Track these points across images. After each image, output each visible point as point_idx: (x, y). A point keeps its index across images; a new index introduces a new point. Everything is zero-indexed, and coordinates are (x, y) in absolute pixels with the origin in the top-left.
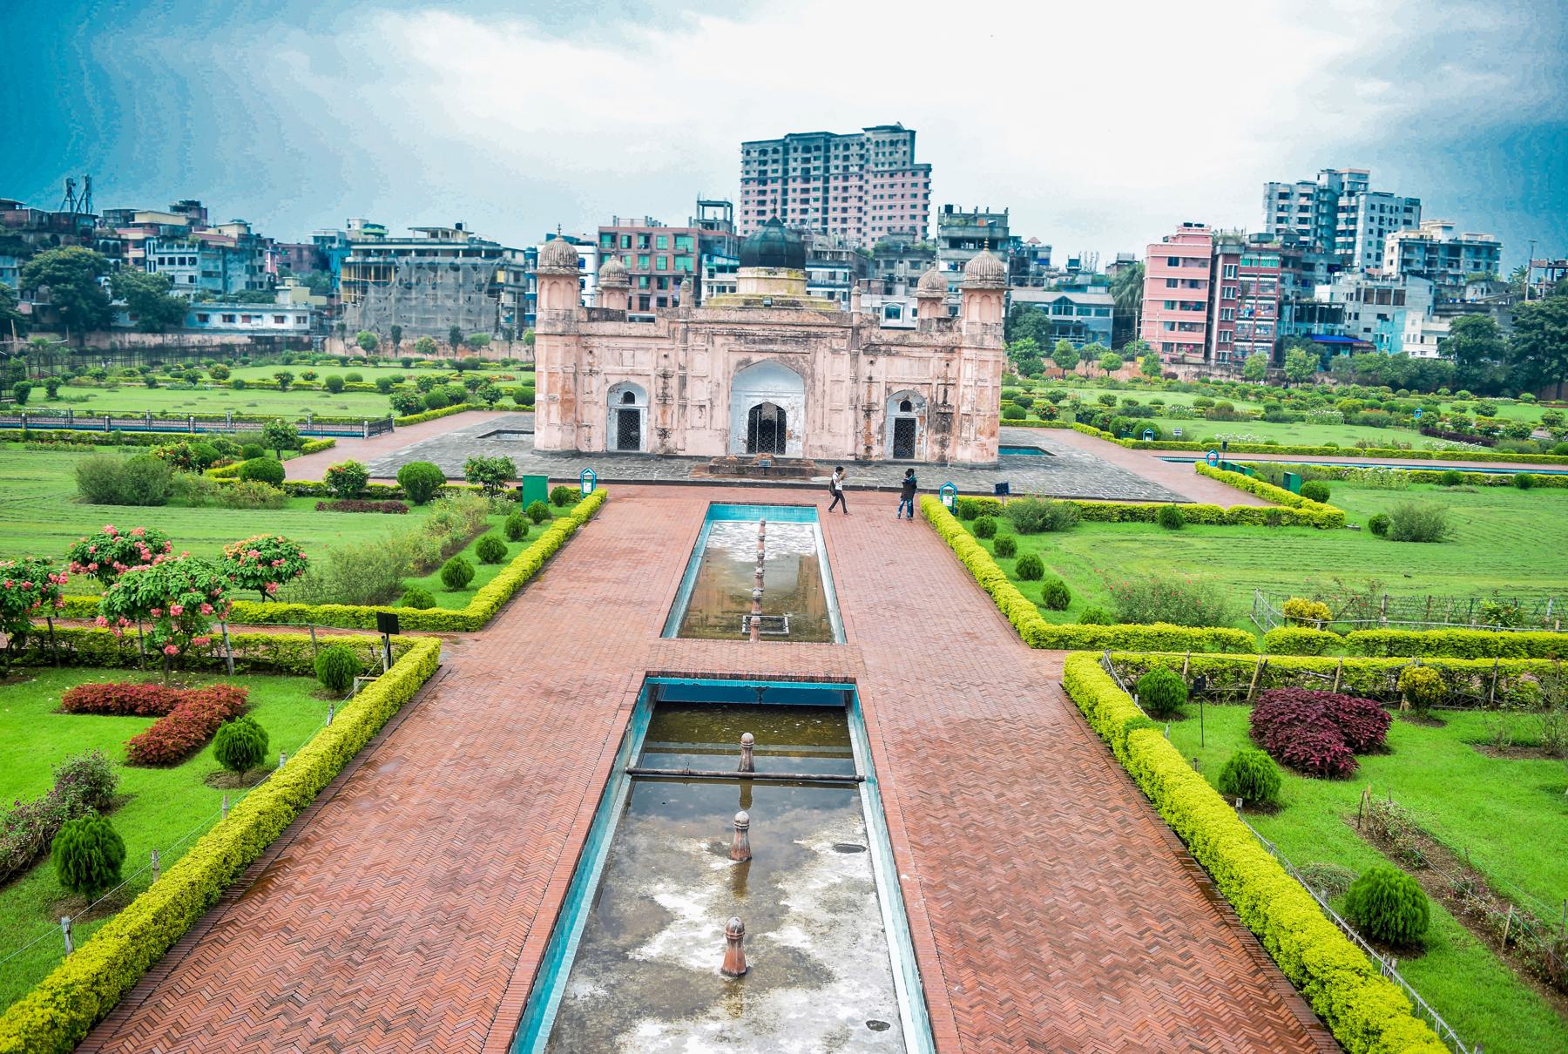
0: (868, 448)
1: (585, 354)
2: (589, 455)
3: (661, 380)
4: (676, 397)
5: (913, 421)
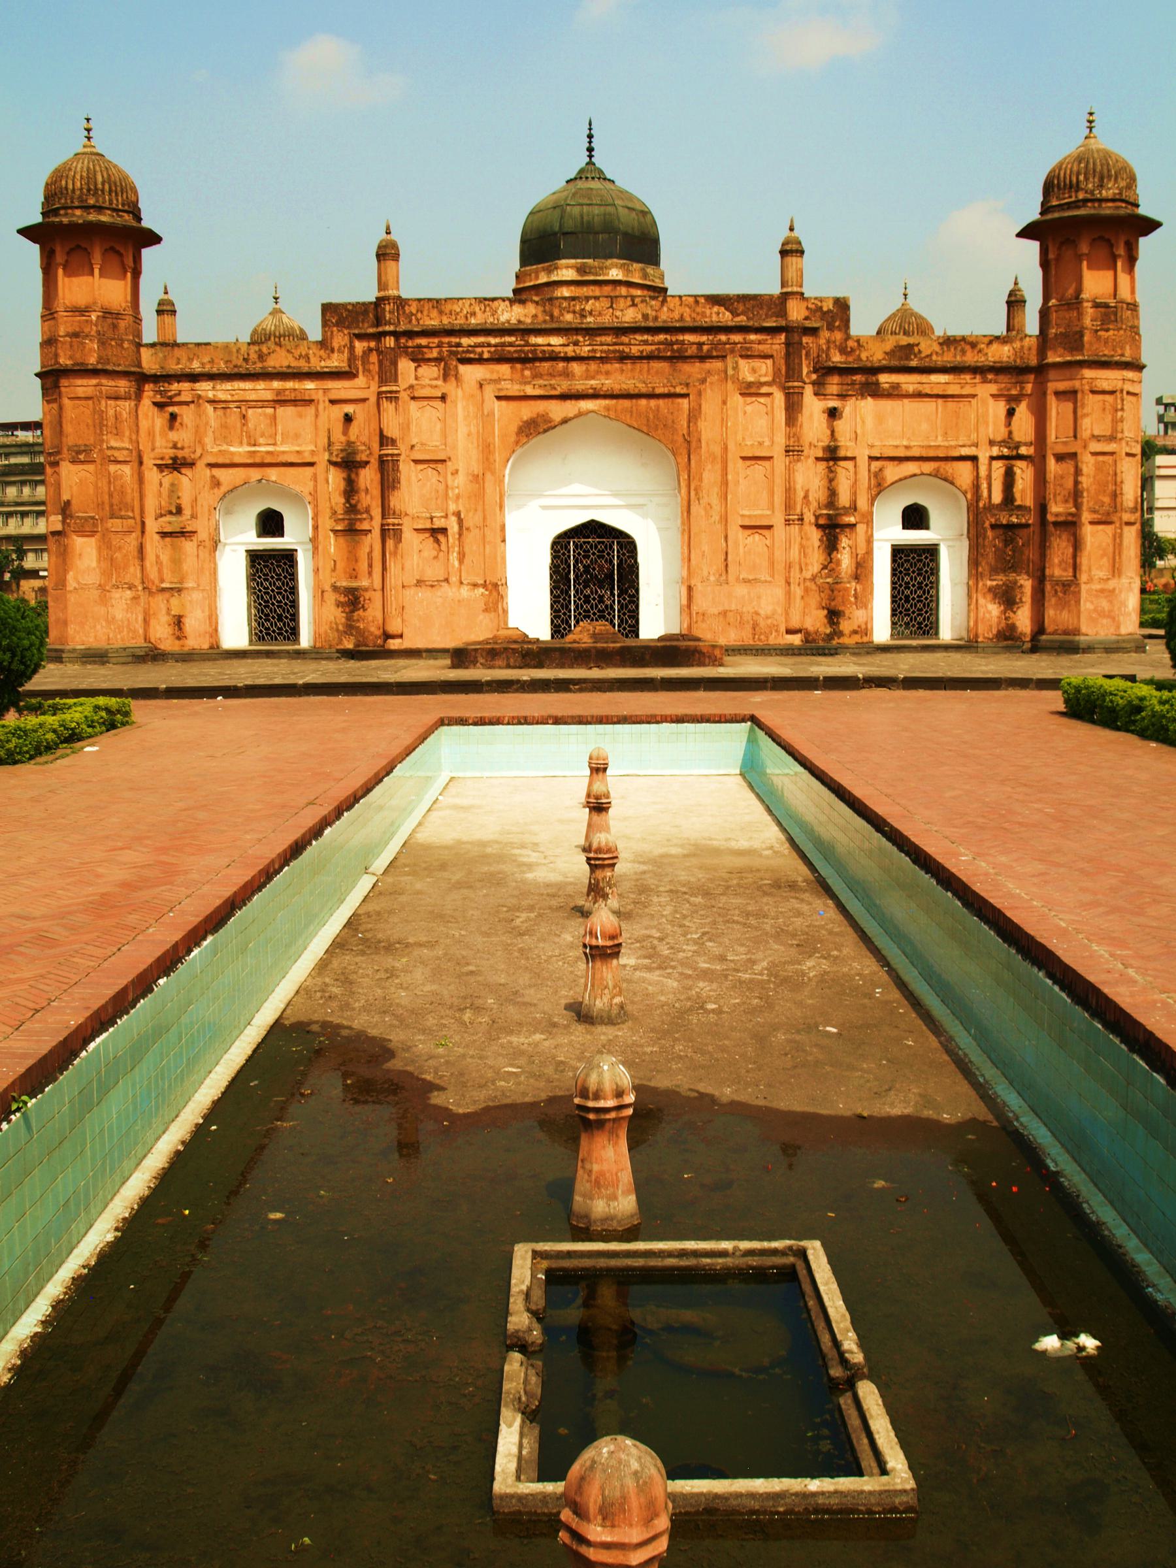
0: (834, 615)
1: (159, 421)
2: (187, 657)
3: (335, 479)
4: (376, 512)
5: (930, 552)
